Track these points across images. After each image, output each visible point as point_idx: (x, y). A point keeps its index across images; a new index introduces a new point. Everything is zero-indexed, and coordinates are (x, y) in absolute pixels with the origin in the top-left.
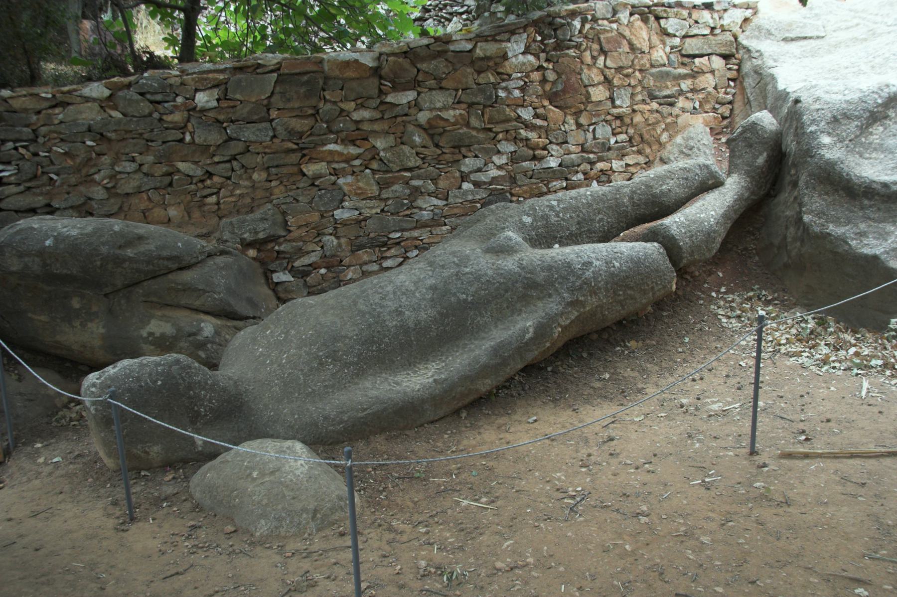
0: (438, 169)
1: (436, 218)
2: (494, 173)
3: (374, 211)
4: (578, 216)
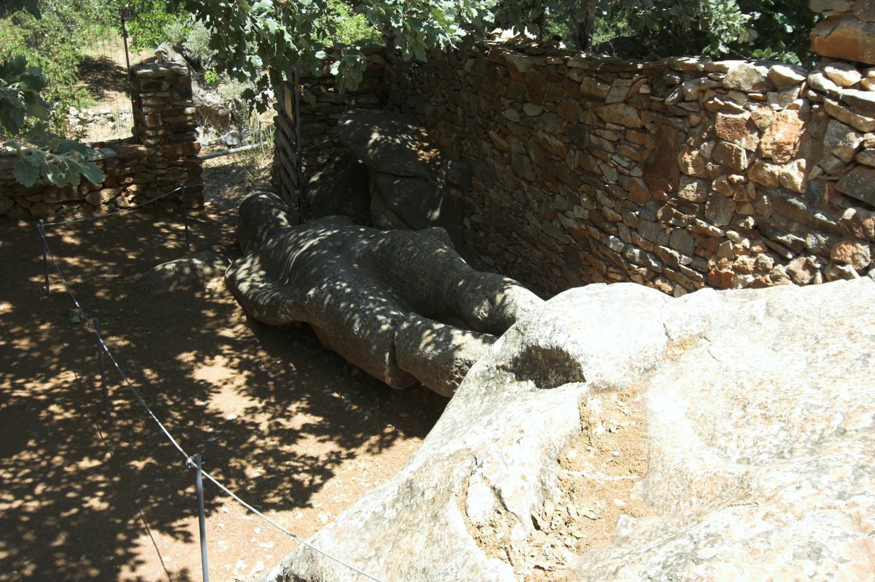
4: (409, 265)
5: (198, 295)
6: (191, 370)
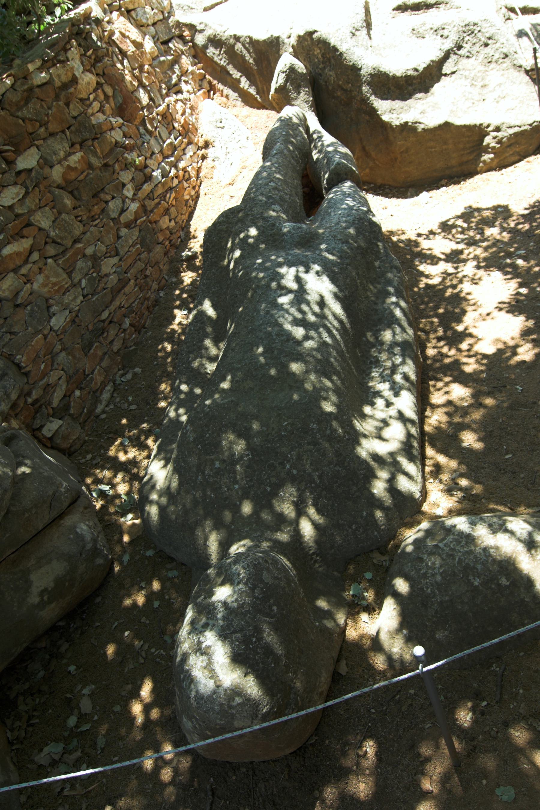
0: (96, 226)
1: (121, 278)
2: (134, 207)
3: (78, 301)
5: (478, 489)
6: (525, 333)
